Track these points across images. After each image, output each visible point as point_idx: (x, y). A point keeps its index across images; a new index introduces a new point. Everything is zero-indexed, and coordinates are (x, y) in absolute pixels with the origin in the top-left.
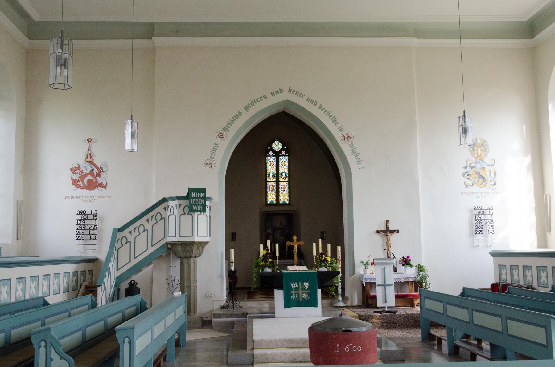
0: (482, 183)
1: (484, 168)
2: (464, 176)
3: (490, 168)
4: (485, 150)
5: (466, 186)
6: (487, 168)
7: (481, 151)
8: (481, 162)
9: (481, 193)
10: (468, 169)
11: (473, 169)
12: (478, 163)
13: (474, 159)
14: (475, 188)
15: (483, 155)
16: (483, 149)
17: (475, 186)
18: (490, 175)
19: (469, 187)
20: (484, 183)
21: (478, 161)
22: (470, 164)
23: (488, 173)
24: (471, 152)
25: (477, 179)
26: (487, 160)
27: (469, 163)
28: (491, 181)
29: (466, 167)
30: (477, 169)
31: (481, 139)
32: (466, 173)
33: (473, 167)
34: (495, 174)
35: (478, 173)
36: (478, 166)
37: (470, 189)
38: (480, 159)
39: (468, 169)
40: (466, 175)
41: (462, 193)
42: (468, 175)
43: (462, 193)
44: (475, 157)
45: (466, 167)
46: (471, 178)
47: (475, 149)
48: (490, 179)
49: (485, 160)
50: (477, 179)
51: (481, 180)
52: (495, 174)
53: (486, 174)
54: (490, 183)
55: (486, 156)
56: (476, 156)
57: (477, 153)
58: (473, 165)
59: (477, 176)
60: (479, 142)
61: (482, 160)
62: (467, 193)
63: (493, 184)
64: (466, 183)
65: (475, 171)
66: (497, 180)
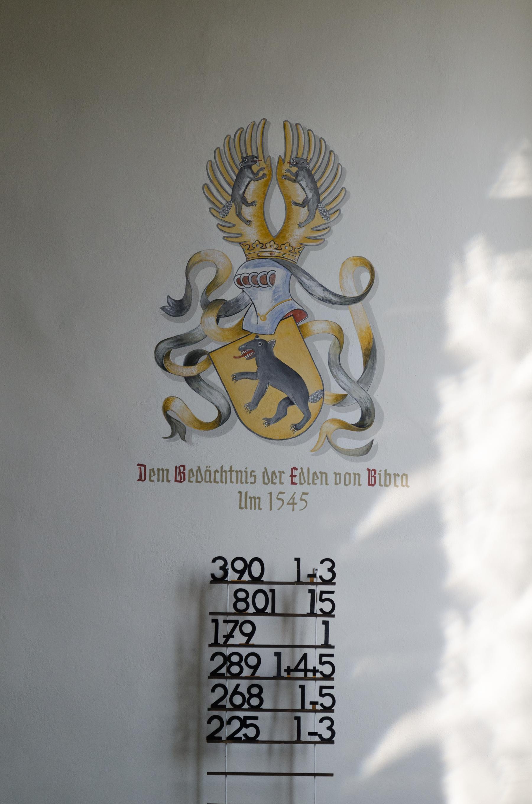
0: (281, 414)
1: (299, 315)
2: (163, 361)
3: (342, 316)
4: (315, 203)
5: (177, 429)
6: (321, 315)
7: (290, 204)
8: (281, 273)
9: (270, 478)
10: (196, 320)
11: (230, 323)
12: (266, 281)
13: (236, 256)
14: (237, 446)
15: (297, 235)
16: (299, 193)
17: (236, 430)
18: (336, 363)
19: (197, 438)
20: (295, 413)
21: (268, 268)
22: (208, 290)
23: (322, 348)
24: (220, 211)
25: (250, 387)
26: (325, 265)
27: (203, 278)
28: (340, 400)
29: (179, 308)
30: (252, 323)
31: (291, 129)
32: (180, 341)
33: (226, 309)
34: (370, 355)
35: (260, 349)
36: (264, 299)
37: (201, 450)
38: (280, 255)
39: (196, 320)
40: (179, 358)
41: (143, 473)
42: (191, 360)
43: (143, 473)
44: (247, 247)
45: (179, 308)
46: (212, 377)
47: (252, 191)
48: (335, 388)
49: (312, 262)
50: (250, 387)
51: (275, 395)
52: (370, 355)
53: (311, 356)
54: (334, 413)
55: (318, 240)
56: (251, 234)
57: (262, 216)
58: (231, 292)
59: (251, 365)
60: (276, 147)
61: (292, 268)
62: (181, 475)
63: (354, 416)
64: (176, 409)
65: (241, 330)
66: (381, 394)
